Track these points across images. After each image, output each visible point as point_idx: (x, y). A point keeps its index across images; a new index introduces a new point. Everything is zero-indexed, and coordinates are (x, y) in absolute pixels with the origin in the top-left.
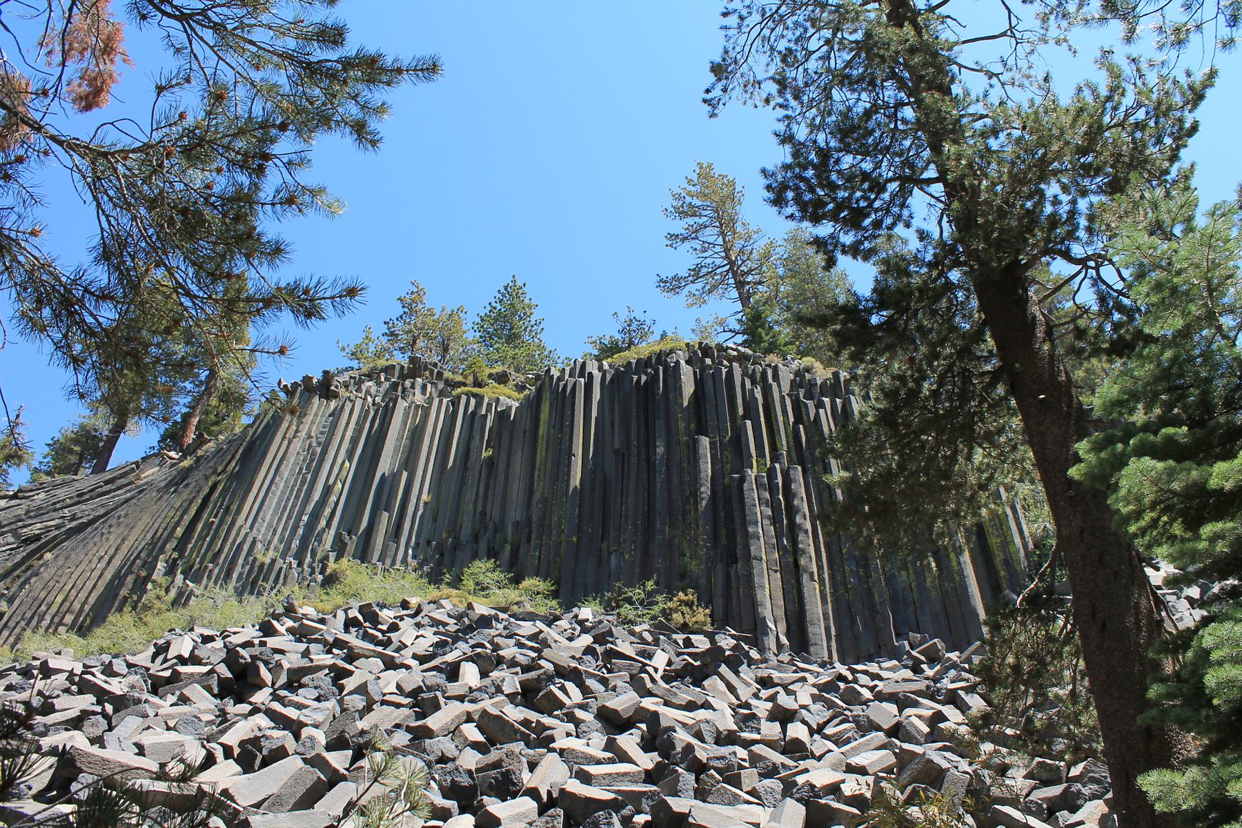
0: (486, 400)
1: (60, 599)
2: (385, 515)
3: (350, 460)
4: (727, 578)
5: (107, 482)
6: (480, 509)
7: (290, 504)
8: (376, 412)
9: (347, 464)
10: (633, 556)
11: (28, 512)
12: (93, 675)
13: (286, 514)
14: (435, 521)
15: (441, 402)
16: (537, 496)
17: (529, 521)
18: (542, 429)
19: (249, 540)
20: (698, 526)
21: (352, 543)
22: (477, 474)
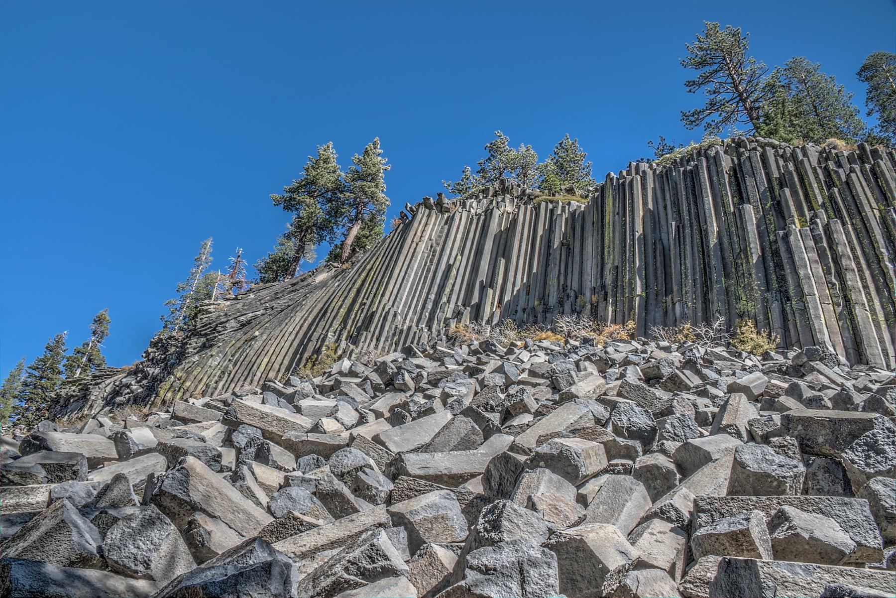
0: (561, 204)
1: (266, 360)
2: (490, 291)
3: (462, 255)
4: (783, 312)
6: (562, 282)
7: (420, 288)
8: (478, 219)
9: (459, 257)
10: (695, 304)
11: (243, 306)
12: (274, 383)
13: (417, 295)
14: (528, 294)
15: (526, 209)
16: (608, 266)
17: (603, 287)
18: (608, 218)
19: (392, 313)
20: (750, 275)
21: (467, 312)
22: (558, 257)
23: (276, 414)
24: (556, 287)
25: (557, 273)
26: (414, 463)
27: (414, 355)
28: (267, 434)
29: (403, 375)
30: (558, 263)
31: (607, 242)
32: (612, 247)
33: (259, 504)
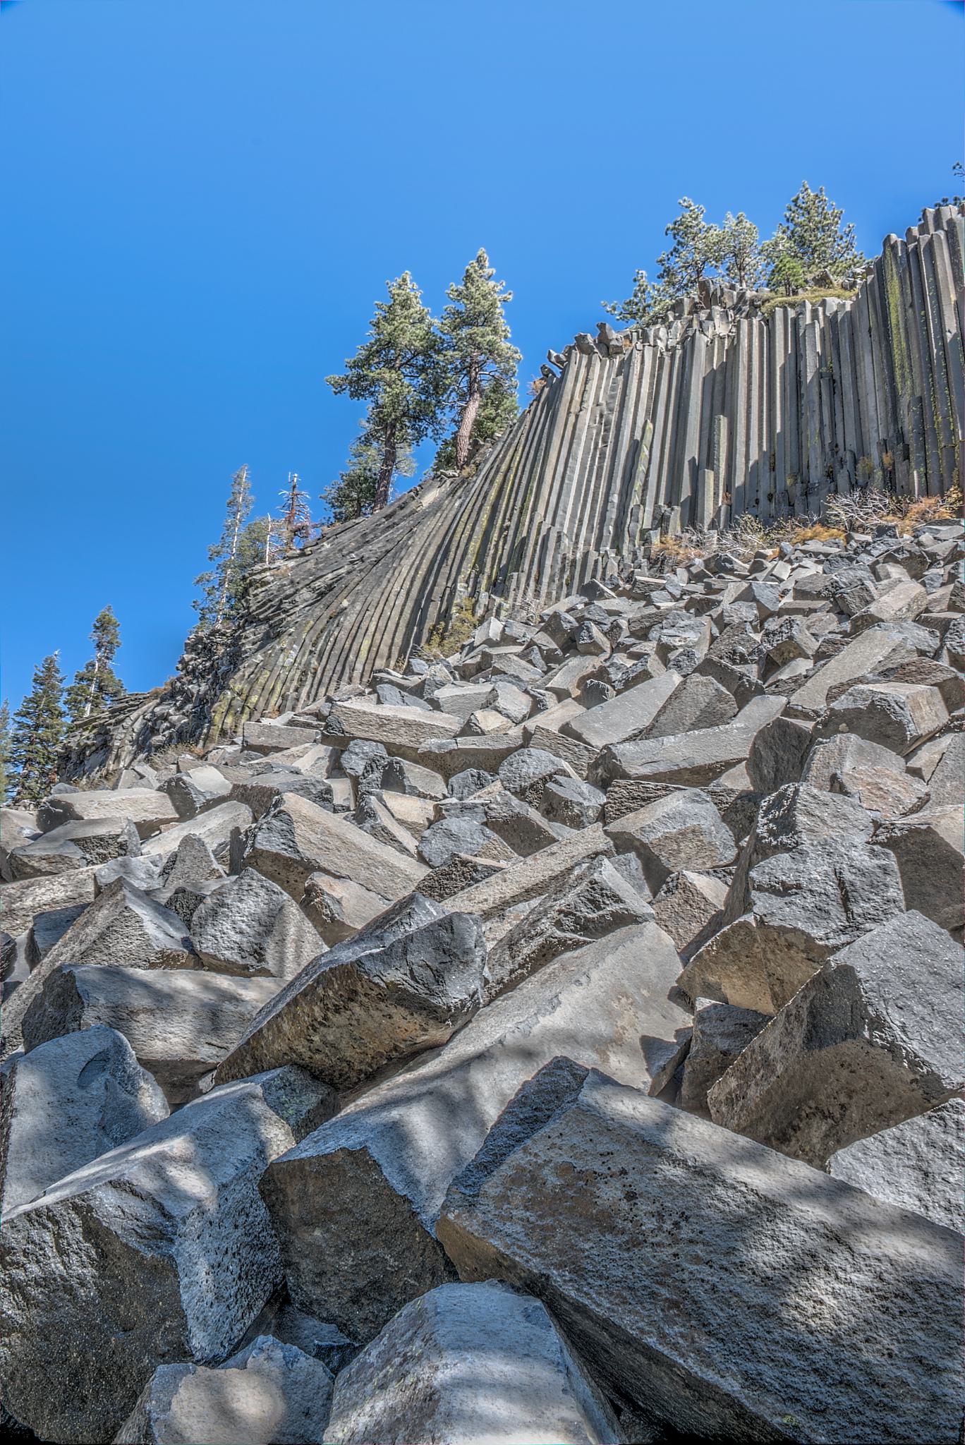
0: (809, 306)
1: (366, 643)
2: (710, 475)
3: (654, 421)
5: (388, 517)
6: (828, 440)
7: (592, 487)
8: (673, 357)
9: (650, 425)
11: (317, 564)
12: (389, 673)
13: (590, 500)
15: (750, 325)
16: (905, 400)
17: (901, 436)
18: (895, 316)
19: (553, 536)
21: (675, 516)
23: (403, 717)
24: (819, 450)
25: (818, 425)
26: (635, 760)
27: (602, 595)
28: (392, 749)
29: (588, 629)
30: (817, 408)
31: (897, 358)
32: (906, 365)
33: (404, 850)
